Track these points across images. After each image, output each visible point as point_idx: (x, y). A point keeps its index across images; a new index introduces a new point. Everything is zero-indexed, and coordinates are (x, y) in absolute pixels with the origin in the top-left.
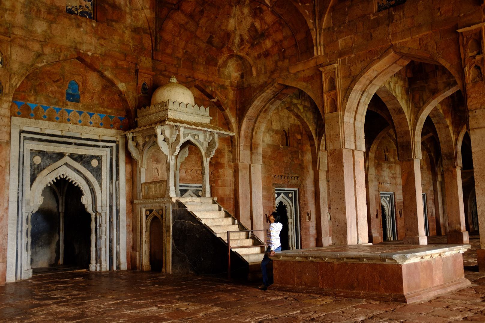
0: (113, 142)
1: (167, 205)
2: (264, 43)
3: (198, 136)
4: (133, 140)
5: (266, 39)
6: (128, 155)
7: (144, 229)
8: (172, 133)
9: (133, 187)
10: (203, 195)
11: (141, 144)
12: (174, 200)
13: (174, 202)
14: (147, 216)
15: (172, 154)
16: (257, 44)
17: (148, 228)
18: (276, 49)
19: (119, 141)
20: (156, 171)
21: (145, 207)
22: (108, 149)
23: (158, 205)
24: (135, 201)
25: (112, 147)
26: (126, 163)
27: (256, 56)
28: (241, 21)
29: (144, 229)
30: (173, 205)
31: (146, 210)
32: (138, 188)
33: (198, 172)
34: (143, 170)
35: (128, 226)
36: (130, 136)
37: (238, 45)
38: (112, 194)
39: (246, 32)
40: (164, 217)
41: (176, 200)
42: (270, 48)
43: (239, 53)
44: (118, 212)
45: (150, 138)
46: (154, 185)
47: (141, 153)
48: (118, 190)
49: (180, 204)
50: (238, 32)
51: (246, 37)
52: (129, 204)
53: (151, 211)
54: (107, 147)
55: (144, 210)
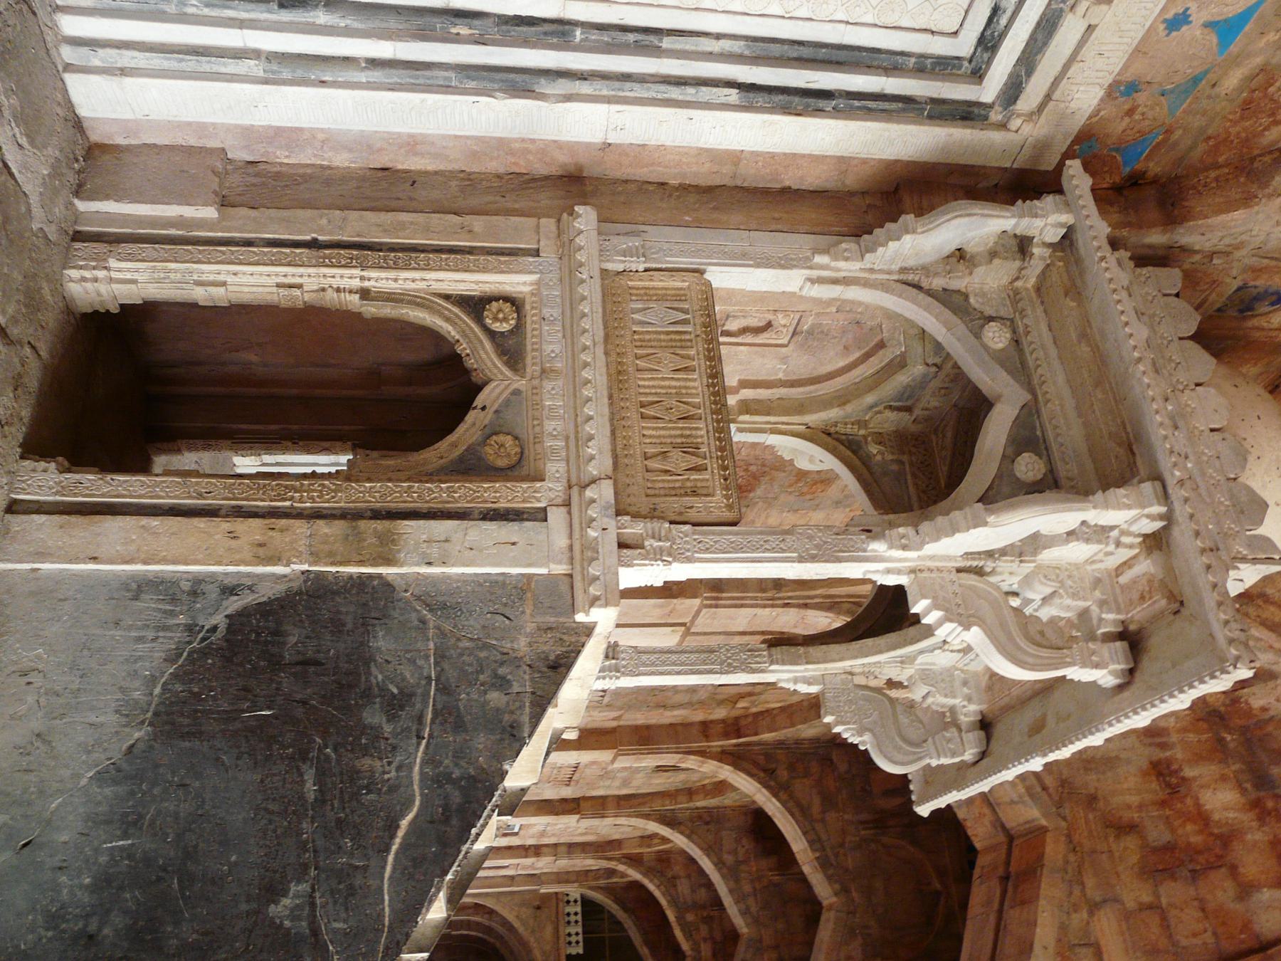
0: (1013, 90)
2: (1224, 778)
5: (1243, 791)
7: (381, 280)
8: (1061, 577)
9: (685, 189)
11: (958, 283)
13: (580, 617)
14: (475, 305)
16: (1221, 741)
17: (388, 311)
18: (1191, 834)
19: (1003, 126)
20: (754, 322)
22: (964, 46)
24: (586, 217)
25: (978, 75)
26: (841, 160)
29: (381, 280)
30: (560, 596)
31: (515, 302)
32: (676, 234)
34: (789, 281)
35: (413, 144)
38: (657, 52)
40: (462, 493)
42: (1198, 805)
44: (518, 83)
45: (1001, 359)
48: (675, 93)
52: (563, 158)
53: (511, 350)
54: (989, 43)
55: (516, 282)
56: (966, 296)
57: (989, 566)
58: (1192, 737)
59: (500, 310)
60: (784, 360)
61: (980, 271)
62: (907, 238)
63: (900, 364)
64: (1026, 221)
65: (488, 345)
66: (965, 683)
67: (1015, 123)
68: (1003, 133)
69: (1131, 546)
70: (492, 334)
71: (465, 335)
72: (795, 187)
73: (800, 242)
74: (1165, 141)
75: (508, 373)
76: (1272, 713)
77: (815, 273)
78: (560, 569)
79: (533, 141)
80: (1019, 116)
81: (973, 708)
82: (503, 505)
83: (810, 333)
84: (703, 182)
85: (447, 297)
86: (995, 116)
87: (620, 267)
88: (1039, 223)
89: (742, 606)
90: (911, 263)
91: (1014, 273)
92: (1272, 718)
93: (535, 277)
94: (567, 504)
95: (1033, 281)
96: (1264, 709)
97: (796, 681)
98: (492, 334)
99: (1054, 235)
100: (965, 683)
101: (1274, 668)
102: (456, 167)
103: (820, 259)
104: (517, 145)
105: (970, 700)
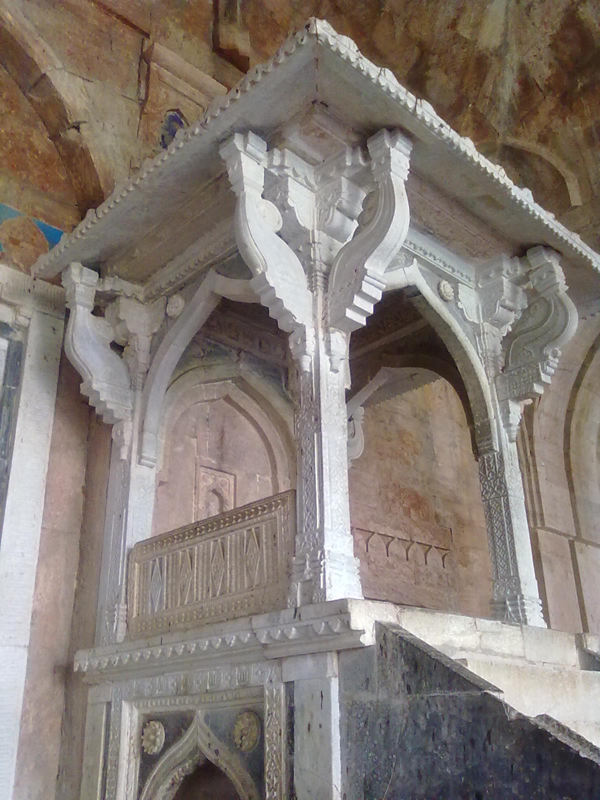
1: (301, 670)
3: (455, 283)
4: (97, 312)
6: (68, 381)
10: (520, 620)
11: (143, 342)
12: (366, 620)
13: (368, 639)
14: (147, 762)
15: (333, 320)
16: (584, 89)
19: (26, 330)
21: (137, 698)
23: (225, 677)
24: (83, 662)
26: (53, 449)
27: (581, 137)
28: (529, 7)
31: (147, 721)
33: (394, 547)
36: (83, 284)
37: (511, 110)
39: (546, 52)
40: (274, 775)
41: (382, 629)
43: (511, 140)
46: (202, 546)
47: (138, 382)
49: (423, 665)
50: (513, 58)
51: (542, 72)
52: (46, 684)
56: (154, 334)
57: (320, 266)
58: (587, 111)
59: (148, 740)
60: (251, 477)
61: (131, 327)
62: (95, 386)
63: (241, 382)
64: (78, 298)
65: (173, 750)
66: (487, 277)
67: (22, 320)
68: (30, 329)
69: (283, 156)
70: (167, 745)
71: (166, 774)
72: (83, 483)
73: (115, 471)
74: (44, 216)
75: (191, 729)
76: (552, 61)
77: (134, 456)
78: (333, 665)
79: (25, 713)
80: (16, 319)
81: (506, 266)
82: (283, 728)
83: (221, 458)
84: (75, 561)
85: (140, 791)
86: (18, 336)
87: (122, 626)
88: (80, 289)
89: (538, 492)
90: (125, 381)
91: (133, 302)
92: (556, 59)
93: (126, 707)
94: (280, 660)
95: (137, 287)
96: (550, 66)
97: (508, 425)
98: (167, 745)
99: (92, 276)
100: (487, 277)
101: (515, 68)
102: (53, 784)
103: (124, 456)
104: (31, 727)
105: (499, 270)
